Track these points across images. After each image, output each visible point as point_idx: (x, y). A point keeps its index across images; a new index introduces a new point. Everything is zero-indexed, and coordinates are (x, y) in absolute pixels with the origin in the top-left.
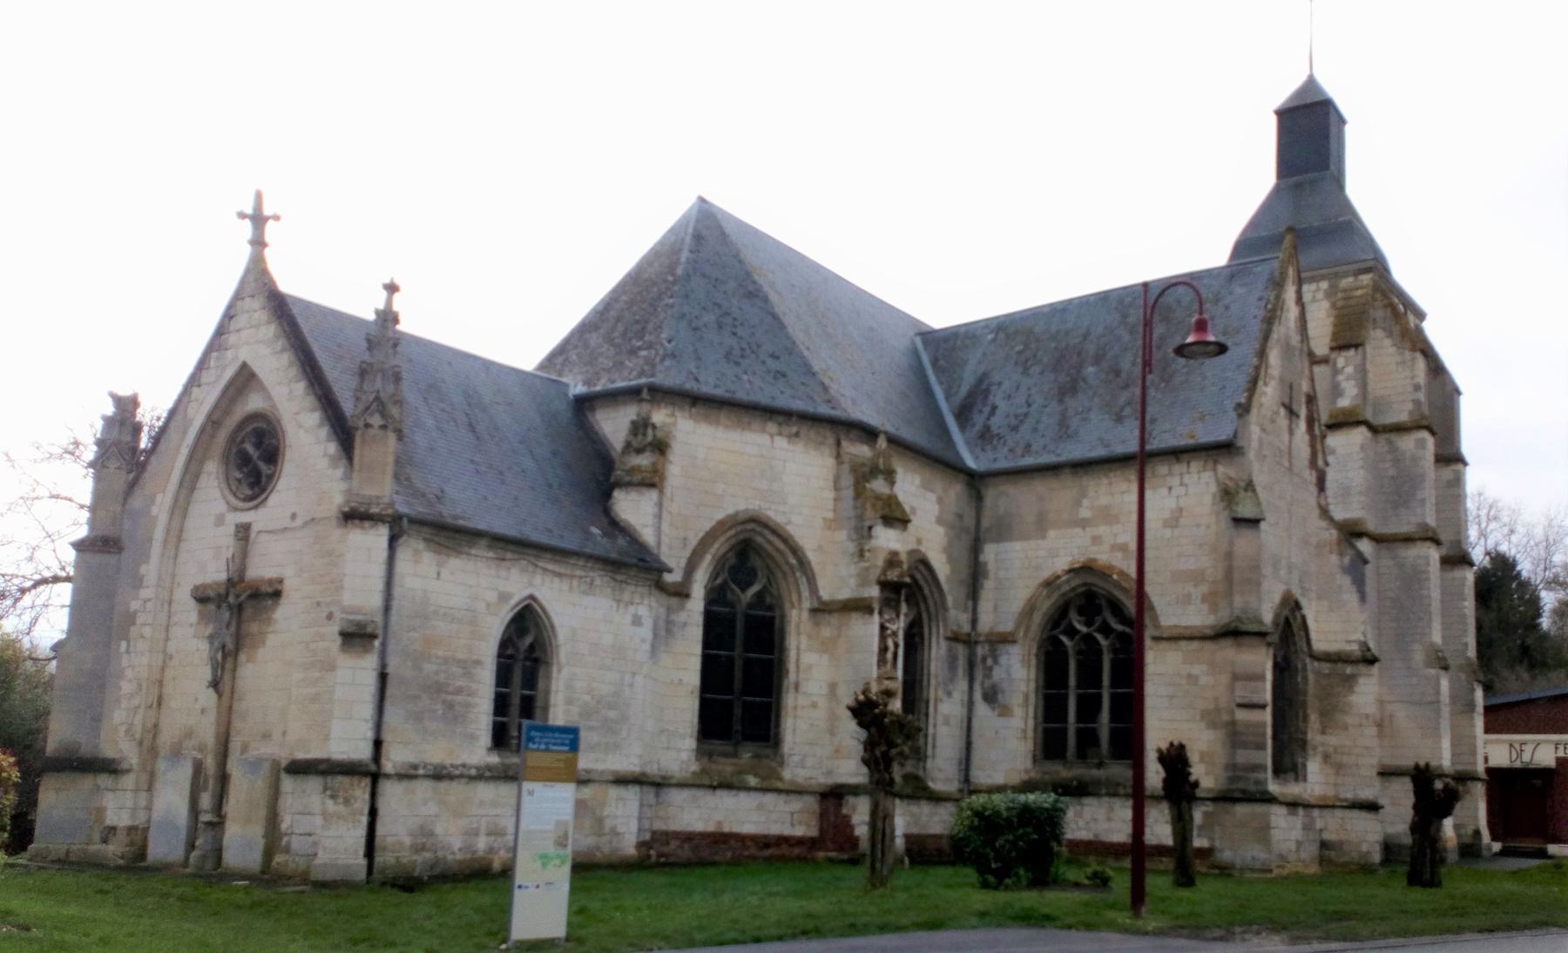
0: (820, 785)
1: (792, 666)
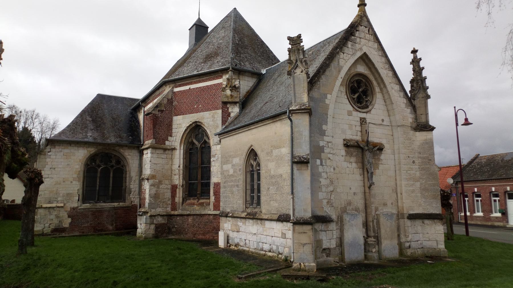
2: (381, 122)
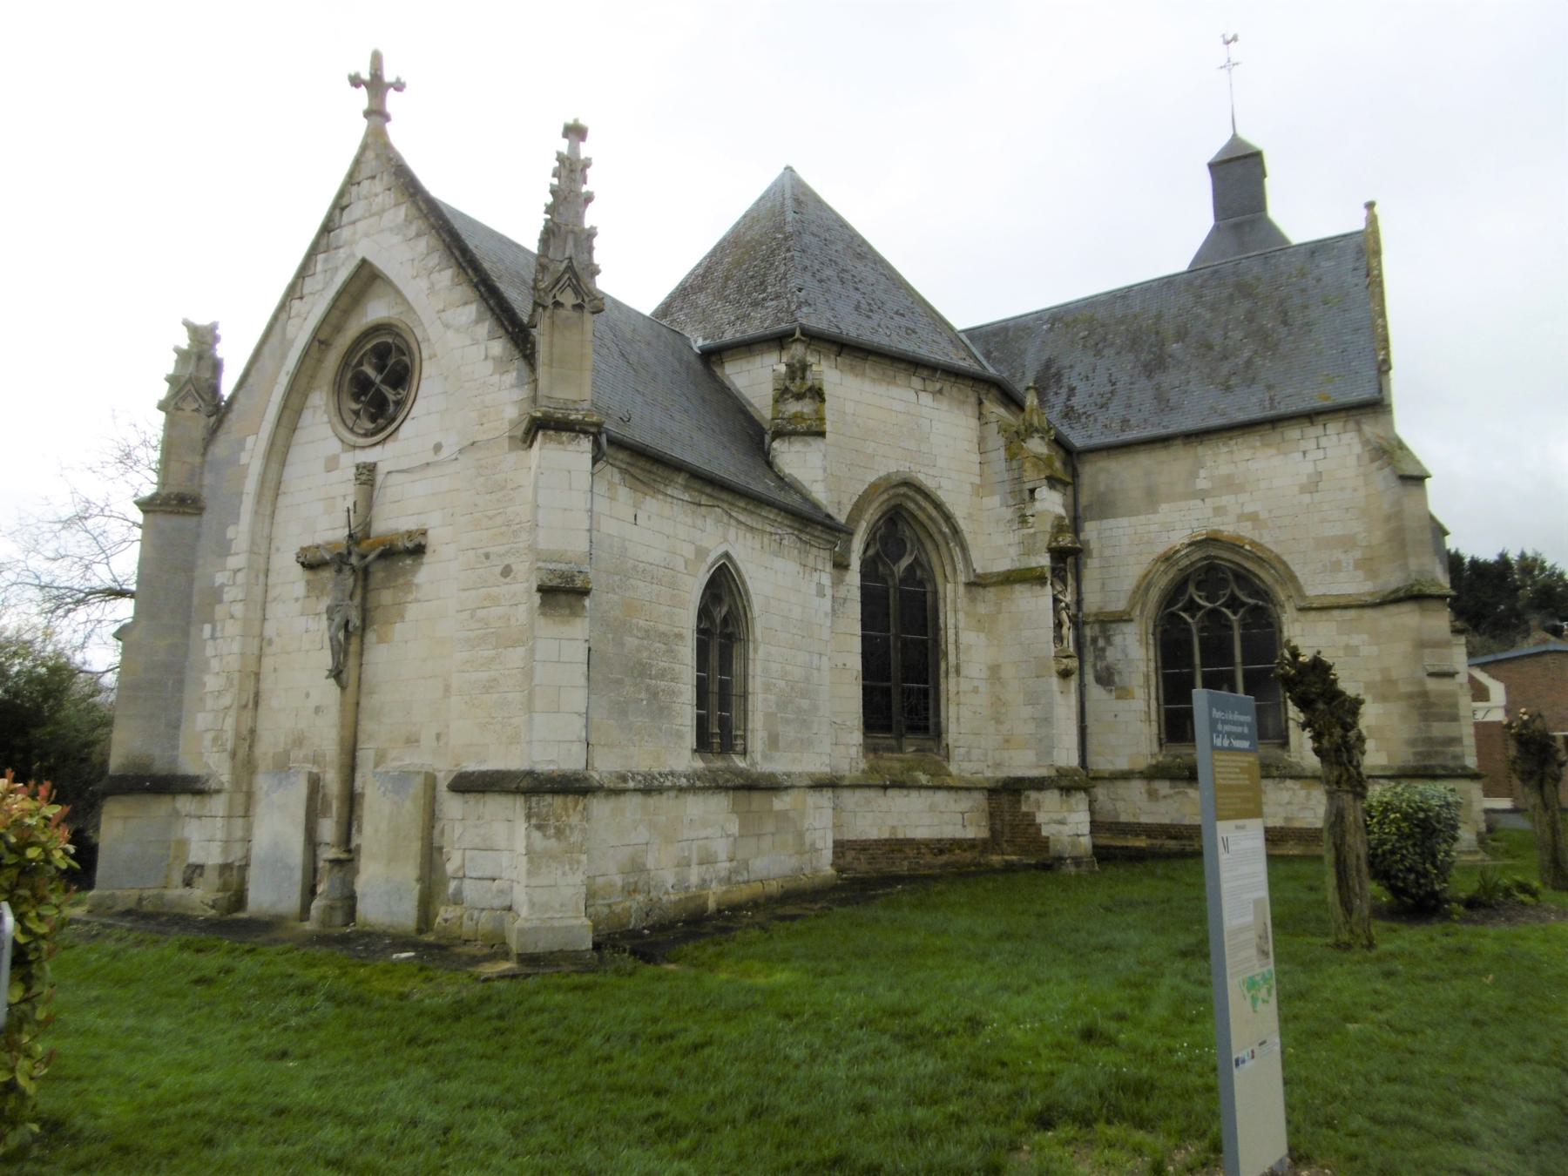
0: (988, 779)
1: (951, 648)
2: (430, 457)
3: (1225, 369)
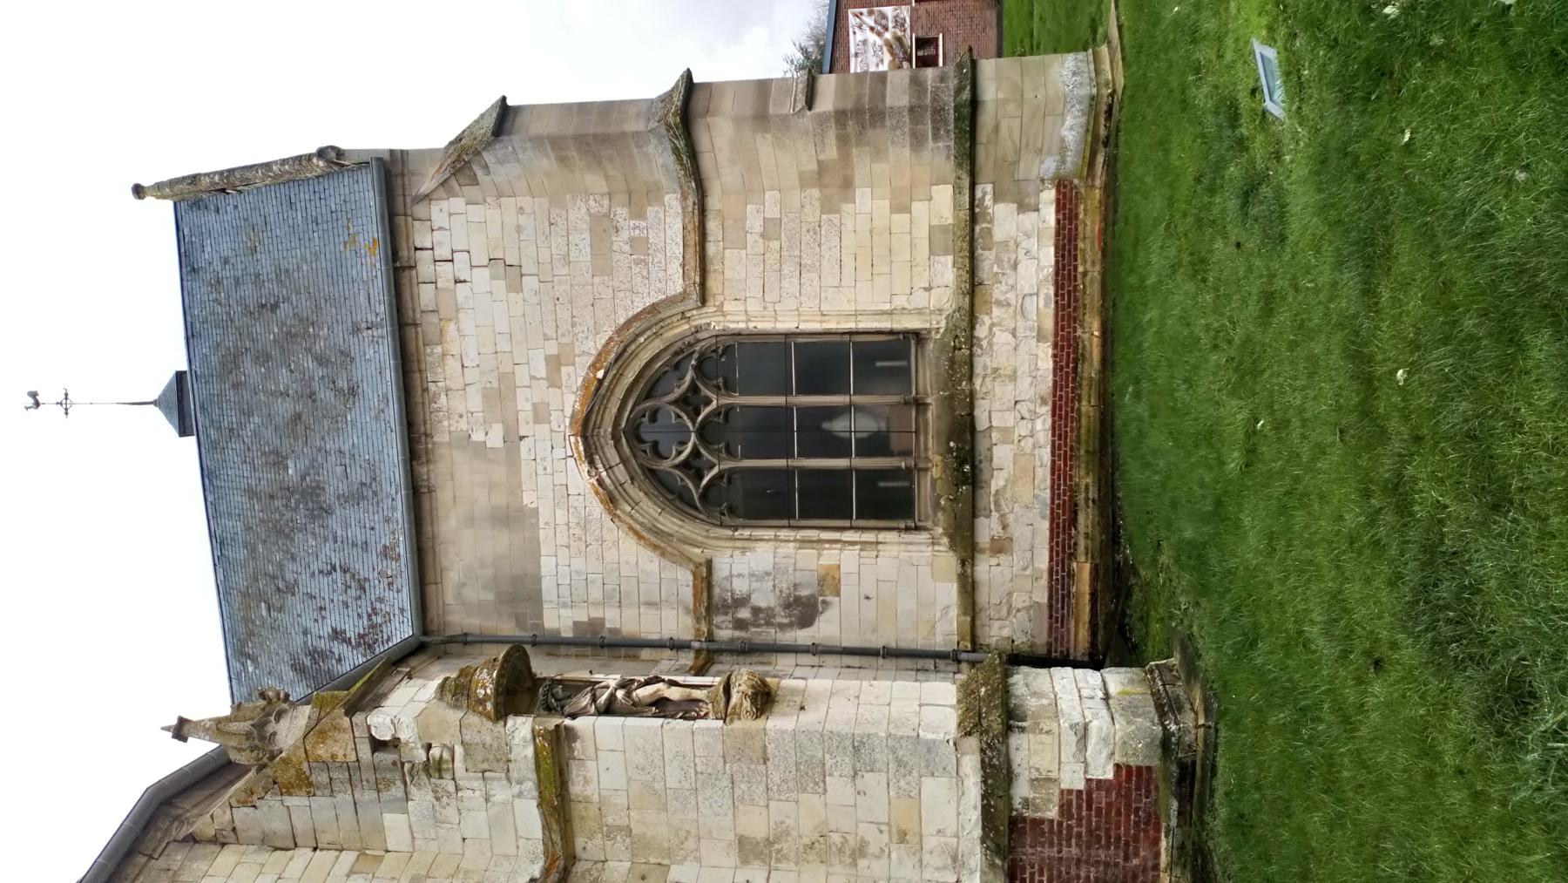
3: (325, 395)
